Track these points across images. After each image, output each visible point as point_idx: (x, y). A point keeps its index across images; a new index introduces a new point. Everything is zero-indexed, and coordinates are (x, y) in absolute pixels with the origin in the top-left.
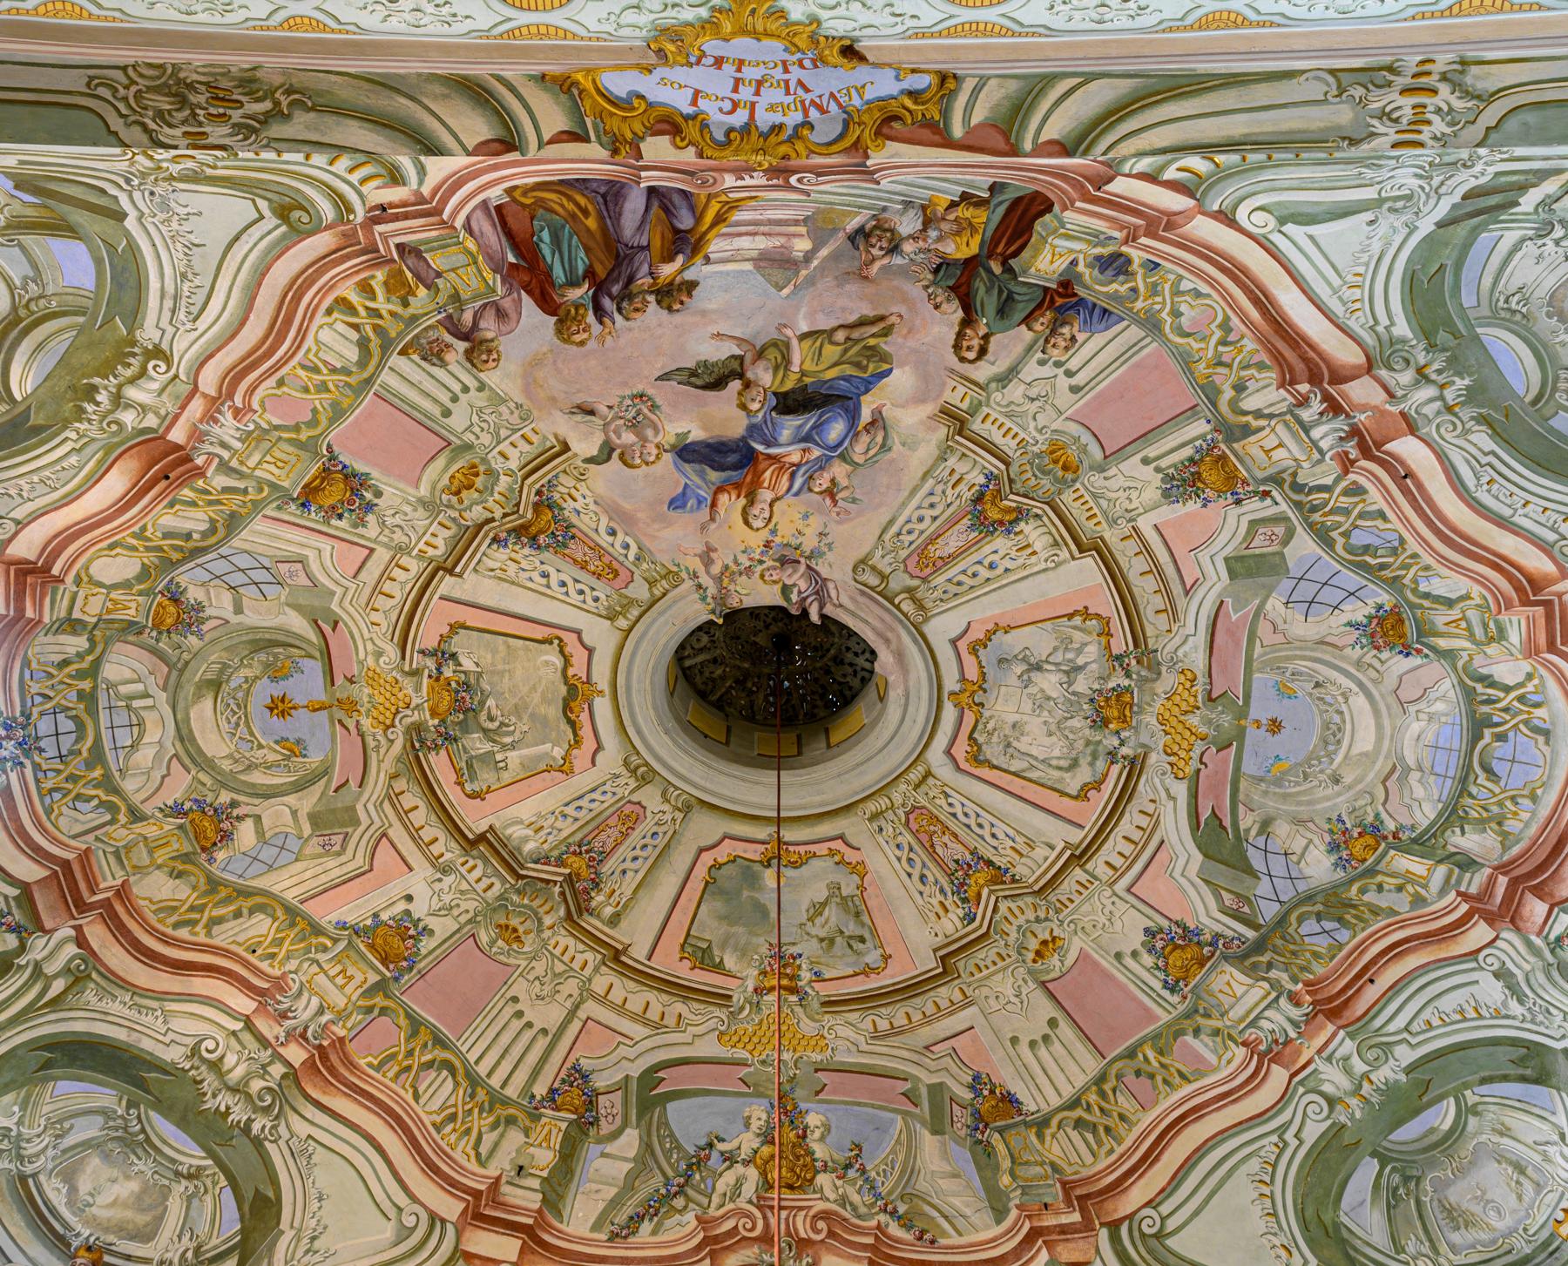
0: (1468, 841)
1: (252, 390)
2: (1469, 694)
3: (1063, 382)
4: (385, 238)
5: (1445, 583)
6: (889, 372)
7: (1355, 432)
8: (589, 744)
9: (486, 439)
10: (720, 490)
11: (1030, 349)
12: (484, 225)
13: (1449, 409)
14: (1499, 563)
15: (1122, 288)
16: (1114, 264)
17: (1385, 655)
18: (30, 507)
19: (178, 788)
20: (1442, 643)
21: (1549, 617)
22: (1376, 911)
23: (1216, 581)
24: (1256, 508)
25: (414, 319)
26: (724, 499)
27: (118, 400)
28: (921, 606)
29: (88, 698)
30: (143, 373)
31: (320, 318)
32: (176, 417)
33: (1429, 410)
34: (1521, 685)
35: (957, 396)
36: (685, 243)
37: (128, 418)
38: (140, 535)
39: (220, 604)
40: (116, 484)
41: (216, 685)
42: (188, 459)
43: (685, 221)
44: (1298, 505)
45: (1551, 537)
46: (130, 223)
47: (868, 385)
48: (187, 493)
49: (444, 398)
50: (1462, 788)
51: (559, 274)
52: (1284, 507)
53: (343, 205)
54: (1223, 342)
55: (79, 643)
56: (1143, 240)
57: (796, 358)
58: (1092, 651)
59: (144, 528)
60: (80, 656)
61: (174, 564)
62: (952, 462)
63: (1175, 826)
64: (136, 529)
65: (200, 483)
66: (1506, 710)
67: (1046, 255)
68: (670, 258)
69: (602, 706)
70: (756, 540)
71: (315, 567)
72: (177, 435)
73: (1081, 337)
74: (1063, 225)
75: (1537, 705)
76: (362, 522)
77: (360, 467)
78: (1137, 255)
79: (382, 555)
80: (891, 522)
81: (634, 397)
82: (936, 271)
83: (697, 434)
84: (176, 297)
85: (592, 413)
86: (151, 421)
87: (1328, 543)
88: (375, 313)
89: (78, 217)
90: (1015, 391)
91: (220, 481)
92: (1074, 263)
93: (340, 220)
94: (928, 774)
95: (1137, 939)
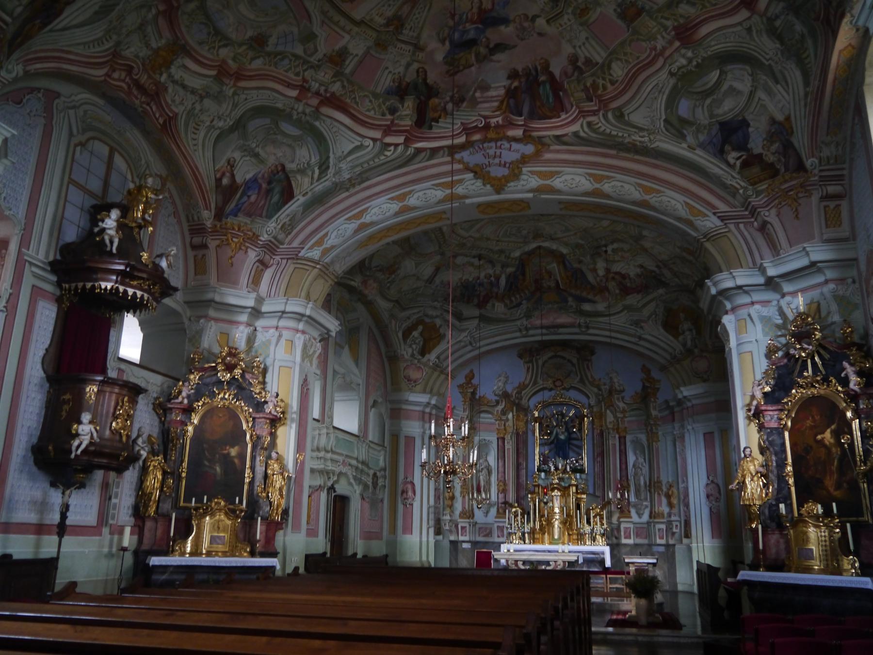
1: (649, 55)
3: (391, 69)
4: (596, 104)
5: (258, 63)
6: (444, 58)
11: (404, 76)
12: (568, 106)
14: (251, 78)
15: (388, 103)
16: (393, 111)
17: (256, 34)
18: (735, 29)
20: (244, 47)
23: (317, 29)
24: (319, 55)
25: (592, 75)
26: (489, 6)
27: (690, 61)
30: (679, 68)
31: (620, 79)
32: (674, 51)
33: (296, 106)
34: (218, 50)
35: (421, 55)
36: (511, 93)
37: (690, 54)
38: (704, 6)
40: (704, 30)
42: (677, 34)
43: (512, 101)
44: (308, 62)
45: (246, 92)
46: (664, 117)
48: (682, 21)
49: (587, 45)
51: (548, 86)
52: (312, 59)
53: (605, 117)
54: (355, 98)
56: (389, 123)
57: (473, 58)
59: (701, 9)
62: (415, 34)
64: (704, 10)
65: (676, 24)
66: (215, 42)
68: (516, 88)
72: (677, 44)
73: (392, 84)
74: (410, 119)
75: (209, 49)
78: (389, 117)
80: (429, 9)
81: (525, 39)
82: (438, 93)
84: (660, 92)
86: (683, 51)
87: (294, 55)
88: (604, 79)
90: (404, 62)
91: (669, 23)
92: (403, 107)
93: (607, 111)
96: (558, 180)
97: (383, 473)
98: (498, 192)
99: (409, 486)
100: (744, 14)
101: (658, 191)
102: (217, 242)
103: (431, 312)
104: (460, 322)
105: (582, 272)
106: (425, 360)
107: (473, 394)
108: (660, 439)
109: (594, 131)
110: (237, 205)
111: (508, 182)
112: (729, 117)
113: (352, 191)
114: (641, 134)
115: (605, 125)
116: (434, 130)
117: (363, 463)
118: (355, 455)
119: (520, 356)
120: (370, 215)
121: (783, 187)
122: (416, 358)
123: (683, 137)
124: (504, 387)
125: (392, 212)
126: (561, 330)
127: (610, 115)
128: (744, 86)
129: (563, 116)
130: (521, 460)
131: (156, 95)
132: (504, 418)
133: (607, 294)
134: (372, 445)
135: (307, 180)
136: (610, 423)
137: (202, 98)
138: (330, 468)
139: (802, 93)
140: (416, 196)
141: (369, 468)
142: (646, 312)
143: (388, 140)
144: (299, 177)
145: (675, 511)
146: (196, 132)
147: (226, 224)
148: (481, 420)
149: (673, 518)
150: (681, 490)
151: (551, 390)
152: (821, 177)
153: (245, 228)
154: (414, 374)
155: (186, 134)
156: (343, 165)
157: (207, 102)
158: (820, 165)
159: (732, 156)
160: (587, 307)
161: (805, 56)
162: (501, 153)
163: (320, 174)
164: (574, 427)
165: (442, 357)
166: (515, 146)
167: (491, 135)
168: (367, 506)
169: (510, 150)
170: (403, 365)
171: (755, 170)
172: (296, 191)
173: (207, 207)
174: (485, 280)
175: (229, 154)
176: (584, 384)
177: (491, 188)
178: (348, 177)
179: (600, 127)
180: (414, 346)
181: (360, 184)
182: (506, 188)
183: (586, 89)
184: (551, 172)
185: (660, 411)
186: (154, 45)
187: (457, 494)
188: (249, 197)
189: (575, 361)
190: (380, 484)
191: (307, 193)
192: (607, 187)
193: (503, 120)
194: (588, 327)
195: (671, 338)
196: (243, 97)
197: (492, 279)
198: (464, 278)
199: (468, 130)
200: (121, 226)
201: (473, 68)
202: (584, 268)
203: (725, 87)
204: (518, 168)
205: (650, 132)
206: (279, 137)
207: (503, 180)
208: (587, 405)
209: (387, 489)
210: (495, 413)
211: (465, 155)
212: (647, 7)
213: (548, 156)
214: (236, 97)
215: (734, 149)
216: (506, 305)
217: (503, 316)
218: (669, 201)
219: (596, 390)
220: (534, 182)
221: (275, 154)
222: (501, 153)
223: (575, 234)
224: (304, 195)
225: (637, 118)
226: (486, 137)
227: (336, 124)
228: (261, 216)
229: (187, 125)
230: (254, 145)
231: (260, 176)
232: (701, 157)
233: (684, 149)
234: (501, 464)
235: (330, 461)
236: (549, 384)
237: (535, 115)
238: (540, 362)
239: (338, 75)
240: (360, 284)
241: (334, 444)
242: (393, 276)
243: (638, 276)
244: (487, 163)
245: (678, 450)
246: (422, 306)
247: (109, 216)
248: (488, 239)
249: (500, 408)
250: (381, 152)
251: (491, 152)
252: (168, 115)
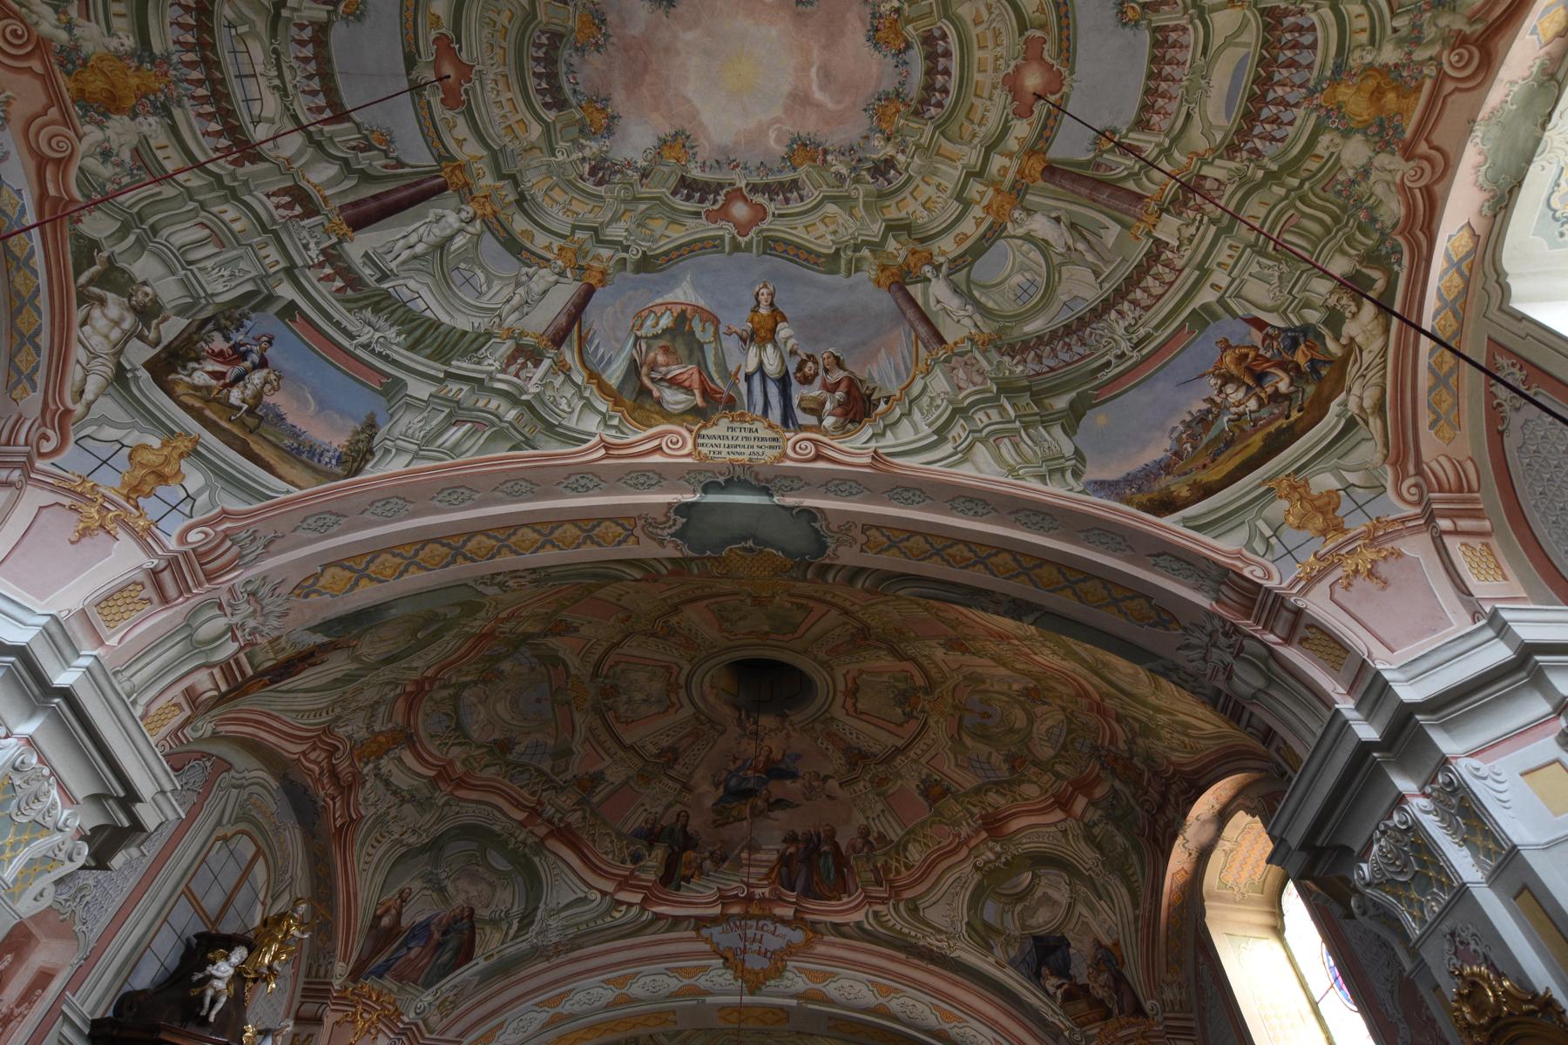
0: (445, 693)
1: (951, 843)
2: (466, 736)
3: (648, 807)
7: (540, 815)
8: (849, 677)
9: (871, 796)
10: (781, 761)
11: (661, 818)
12: (852, 887)
13: (511, 835)
14: (474, 787)
16: (636, 858)
18: (1049, 830)
19: (1040, 709)
20: (484, 750)
21: (449, 776)
22: (476, 663)
24: (568, 776)
26: (779, 757)
27: (998, 856)
28: (697, 719)
29: (1064, 747)
30: (986, 863)
35: (688, 797)
36: (784, 860)
37: (998, 849)
39: (997, 759)
40: (1015, 825)
41: (1011, 730)
42: (984, 824)
43: (784, 870)
44: (552, 781)
46: (966, 920)
47: (721, 800)
49: (882, 819)
50: (456, 709)
51: (830, 860)
55: (1058, 768)
58: (622, 709)
60: (1060, 763)
61: (1005, 782)
63: (574, 662)
67: (660, 856)
69: (841, 686)
70: (767, 742)
71: (953, 762)
72: (984, 835)
76: (928, 776)
77: (921, 799)
78: (629, 865)
79: (923, 761)
83: (788, 782)
85: (828, 796)
86: (991, 844)
87: (538, 770)
88: (898, 861)
89: (980, 927)
91: (976, 810)
93: (898, 902)
94: (690, 661)
95: (582, 628)
96: (833, 985)
98: (752, 993)
100: (1058, 815)
101: (961, 1020)
102: (339, 1016)
109: (881, 924)
110: (387, 961)
112: (1043, 931)
113: (555, 961)
115: (896, 920)
116: (683, 892)
121: (1120, 1034)
123: (990, 948)
125: (604, 1001)
127: (902, 907)
128: (1061, 895)
129: (845, 900)
131: (346, 787)
135: (498, 936)
137: (403, 801)
139: (1131, 916)
140: (641, 982)
143: (622, 896)
144: (488, 930)
146: (375, 844)
147: (362, 988)
152: (1167, 1026)
153: (386, 998)
155: (362, 845)
156: (553, 923)
157: (408, 808)
158: (1164, 1011)
159: (1051, 982)
161: (1130, 872)
163: (519, 929)
166: (781, 929)
167: (754, 910)
171: (1082, 1006)
172: (478, 951)
173: (345, 959)
175: (405, 884)
178: (555, 940)
181: (567, 952)
183: (876, 870)
184: (824, 972)
186: (377, 729)
188: (410, 949)
191: (492, 955)
192: (894, 1005)
193: (770, 893)
196: (458, 809)
199: (724, 899)
200: (239, 976)
201: (745, 823)
203: (1039, 893)
204: (782, 960)
205: (950, 937)
206: (480, 869)
211: (716, 931)
212: (953, 789)
213: (821, 949)
214: (446, 808)
215: (1052, 975)
220: (801, 984)
221: (467, 892)
224: (486, 959)
225: (934, 915)
226: (747, 912)
227: (559, 863)
228: (415, 982)
229: (368, 833)
230: (444, 876)
231: (435, 920)
232: (1011, 977)
233: (990, 964)
237: (809, 892)
239: (582, 803)
247: (227, 958)
250: (608, 912)
252: (350, 816)
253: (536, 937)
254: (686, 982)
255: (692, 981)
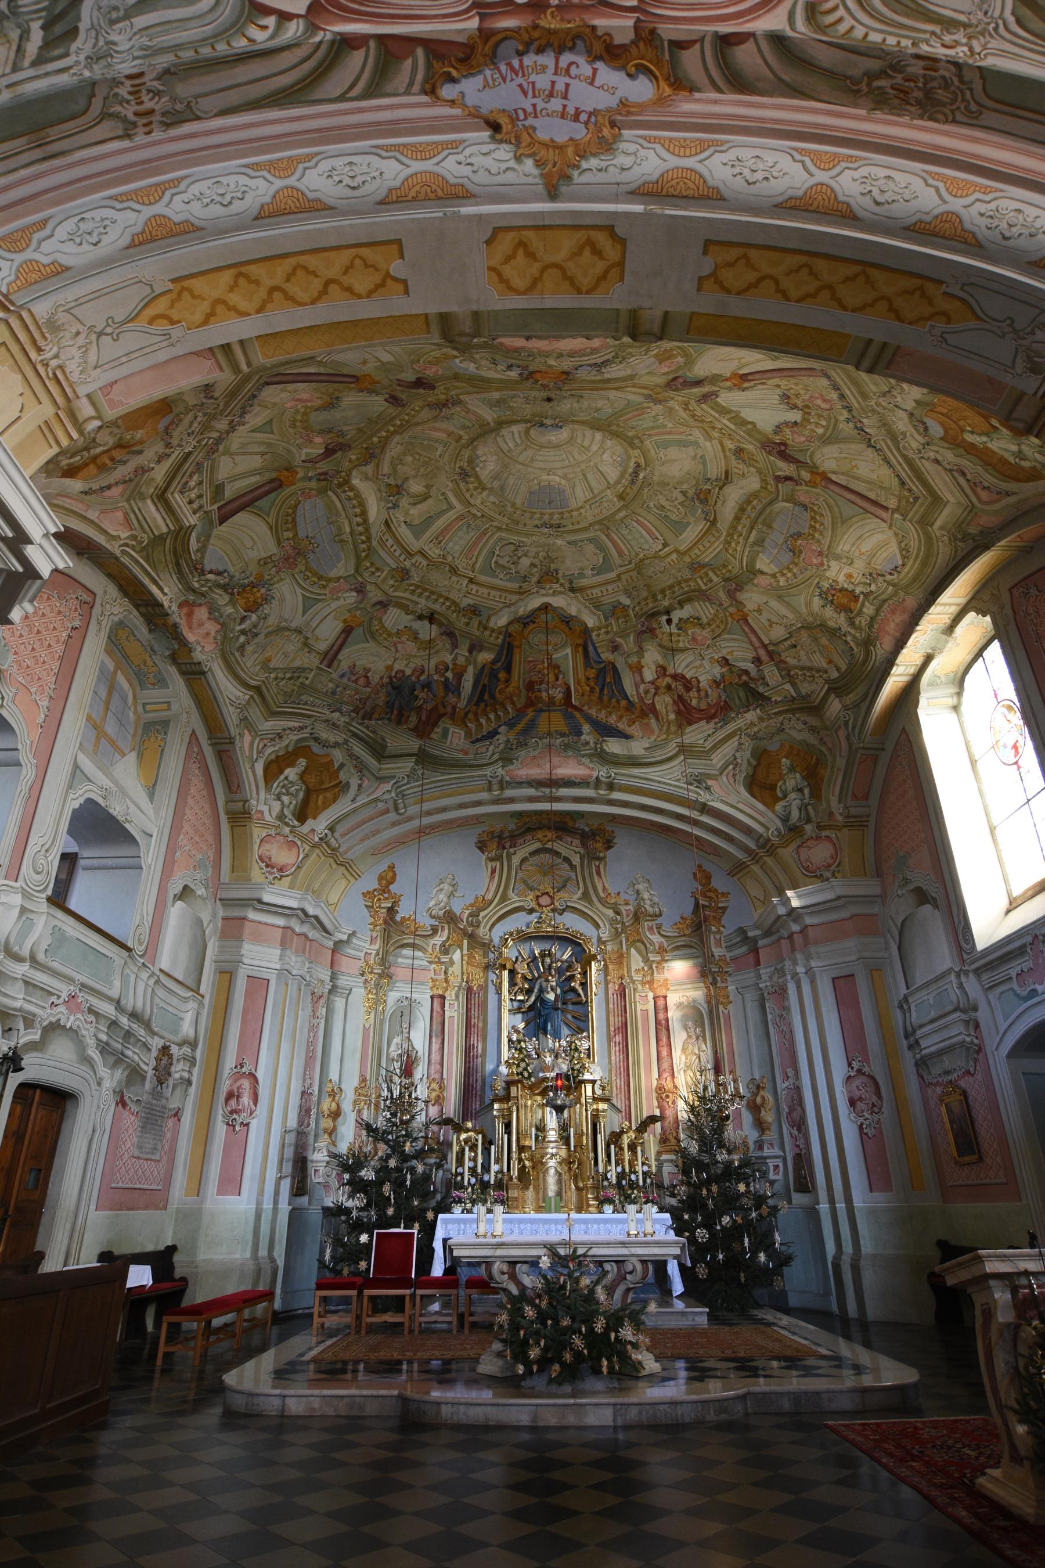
97: (187, 1050)
98: (553, 195)
99: (246, 1083)
103: (324, 735)
104: (379, 761)
105: (615, 669)
106: (305, 829)
107: (392, 911)
108: (731, 998)
111: (583, 154)
114: (948, 38)
117: (134, 1015)
118: (115, 993)
119: (482, 846)
120: (185, 197)
122: (287, 824)
124: (449, 902)
126: (563, 792)
130: (474, 1039)
132: (445, 959)
133: (653, 721)
134: (164, 979)
136: (637, 971)
138: (18, 1004)
141: (154, 1033)
142: (718, 759)
145: (772, 1135)
148: (400, 960)
149: (767, 1152)
150: (782, 1094)
151: (531, 911)
154: (283, 856)
156: (121, 38)
160: (614, 746)
162: (567, 85)
164: (572, 978)
165: (340, 830)
166: (607, 75)
168: (131, 1121)
169: (592, 83)
170: (258, 833)
174: (436, 677)
176: (591, 902)
177: (536, 172)
179: (840, 20)
180: (286, 799)
182: (575, 173)
185: (729, 948)
187: (347, 1106)
189: (576, 860)
190: (177, 1076)
194: (611, 787)
195: (760, 806)
197: (449, 675)
198: (397, 667)
202: (620, 664)
204: (613, 124)
207: (570, 151)
208: (595, 940)
209: (192, 1090)
210: (430, 950)
216: (468, 734)
217: (461, 756)
218: (1019, 211)
219: (610, 913)
222: (567, 85)
223: (619, 576)
234: (435, 1047)
235: (21, 984)
236: (529, 901)
238: (516, 860)
240: (174, 608)
241: (44, 946)
242: (254, 617)
243: (716, 683)
244: (530, 109)
245: (769, 1017)
246: (310, 717)
248: (454, 570)
249: (438, 940)
251: (542, 81)
253: (89, 66)
254: (417, 166)
255: (428, 165)
